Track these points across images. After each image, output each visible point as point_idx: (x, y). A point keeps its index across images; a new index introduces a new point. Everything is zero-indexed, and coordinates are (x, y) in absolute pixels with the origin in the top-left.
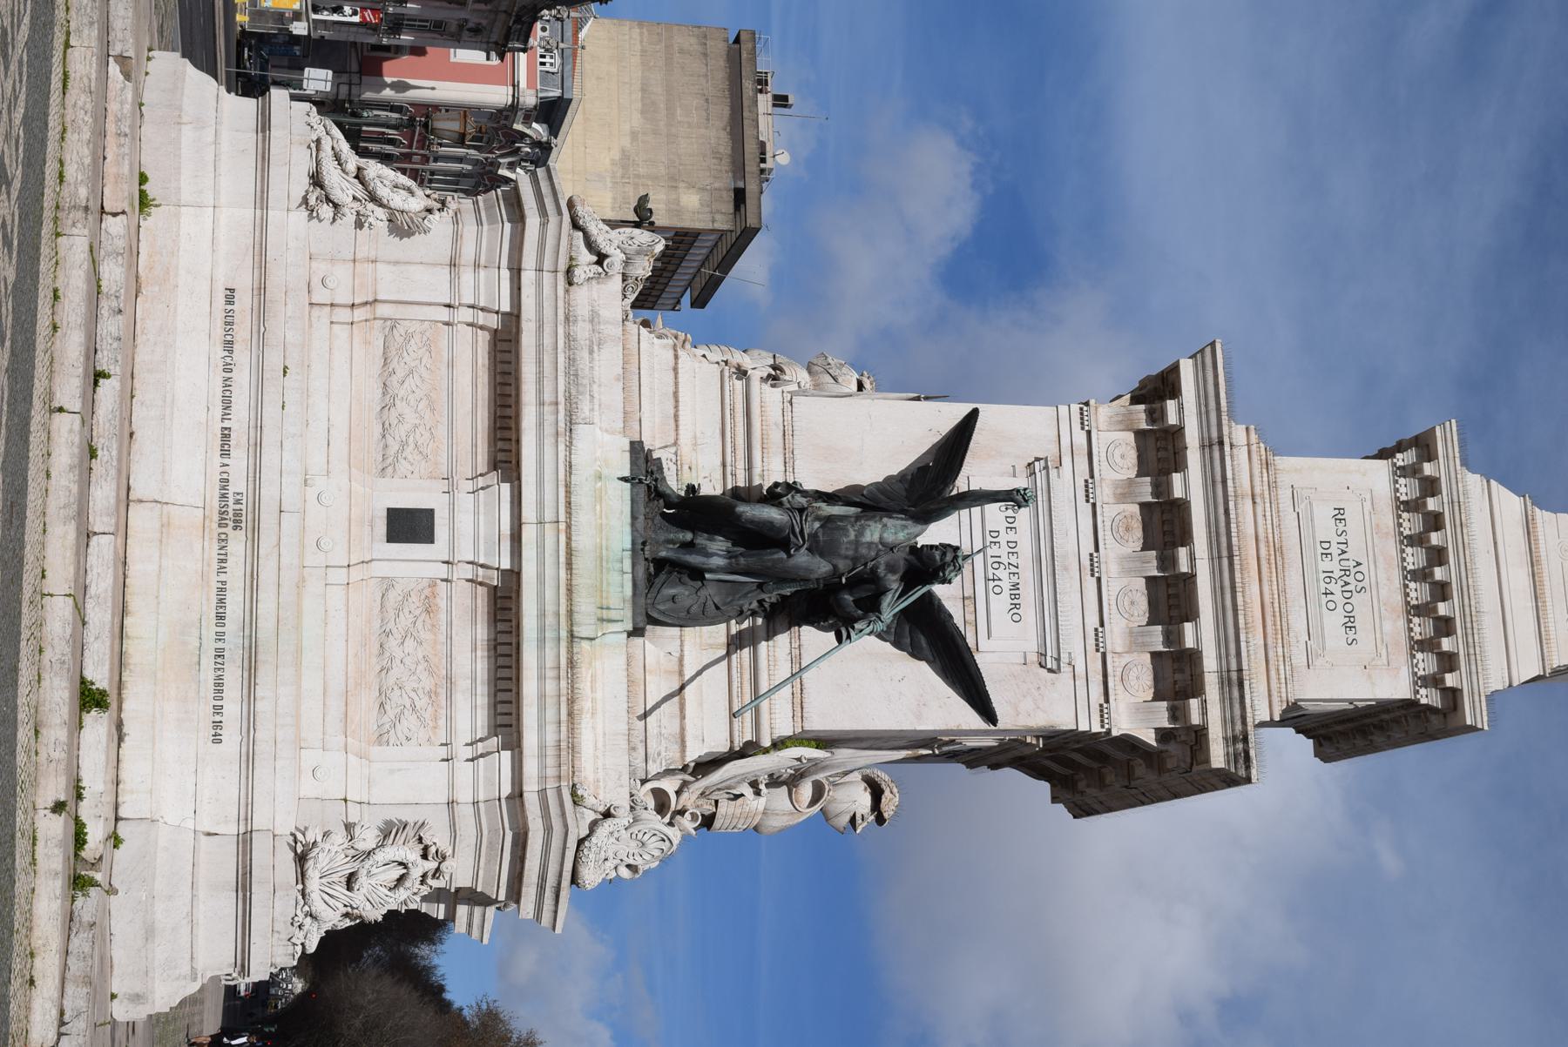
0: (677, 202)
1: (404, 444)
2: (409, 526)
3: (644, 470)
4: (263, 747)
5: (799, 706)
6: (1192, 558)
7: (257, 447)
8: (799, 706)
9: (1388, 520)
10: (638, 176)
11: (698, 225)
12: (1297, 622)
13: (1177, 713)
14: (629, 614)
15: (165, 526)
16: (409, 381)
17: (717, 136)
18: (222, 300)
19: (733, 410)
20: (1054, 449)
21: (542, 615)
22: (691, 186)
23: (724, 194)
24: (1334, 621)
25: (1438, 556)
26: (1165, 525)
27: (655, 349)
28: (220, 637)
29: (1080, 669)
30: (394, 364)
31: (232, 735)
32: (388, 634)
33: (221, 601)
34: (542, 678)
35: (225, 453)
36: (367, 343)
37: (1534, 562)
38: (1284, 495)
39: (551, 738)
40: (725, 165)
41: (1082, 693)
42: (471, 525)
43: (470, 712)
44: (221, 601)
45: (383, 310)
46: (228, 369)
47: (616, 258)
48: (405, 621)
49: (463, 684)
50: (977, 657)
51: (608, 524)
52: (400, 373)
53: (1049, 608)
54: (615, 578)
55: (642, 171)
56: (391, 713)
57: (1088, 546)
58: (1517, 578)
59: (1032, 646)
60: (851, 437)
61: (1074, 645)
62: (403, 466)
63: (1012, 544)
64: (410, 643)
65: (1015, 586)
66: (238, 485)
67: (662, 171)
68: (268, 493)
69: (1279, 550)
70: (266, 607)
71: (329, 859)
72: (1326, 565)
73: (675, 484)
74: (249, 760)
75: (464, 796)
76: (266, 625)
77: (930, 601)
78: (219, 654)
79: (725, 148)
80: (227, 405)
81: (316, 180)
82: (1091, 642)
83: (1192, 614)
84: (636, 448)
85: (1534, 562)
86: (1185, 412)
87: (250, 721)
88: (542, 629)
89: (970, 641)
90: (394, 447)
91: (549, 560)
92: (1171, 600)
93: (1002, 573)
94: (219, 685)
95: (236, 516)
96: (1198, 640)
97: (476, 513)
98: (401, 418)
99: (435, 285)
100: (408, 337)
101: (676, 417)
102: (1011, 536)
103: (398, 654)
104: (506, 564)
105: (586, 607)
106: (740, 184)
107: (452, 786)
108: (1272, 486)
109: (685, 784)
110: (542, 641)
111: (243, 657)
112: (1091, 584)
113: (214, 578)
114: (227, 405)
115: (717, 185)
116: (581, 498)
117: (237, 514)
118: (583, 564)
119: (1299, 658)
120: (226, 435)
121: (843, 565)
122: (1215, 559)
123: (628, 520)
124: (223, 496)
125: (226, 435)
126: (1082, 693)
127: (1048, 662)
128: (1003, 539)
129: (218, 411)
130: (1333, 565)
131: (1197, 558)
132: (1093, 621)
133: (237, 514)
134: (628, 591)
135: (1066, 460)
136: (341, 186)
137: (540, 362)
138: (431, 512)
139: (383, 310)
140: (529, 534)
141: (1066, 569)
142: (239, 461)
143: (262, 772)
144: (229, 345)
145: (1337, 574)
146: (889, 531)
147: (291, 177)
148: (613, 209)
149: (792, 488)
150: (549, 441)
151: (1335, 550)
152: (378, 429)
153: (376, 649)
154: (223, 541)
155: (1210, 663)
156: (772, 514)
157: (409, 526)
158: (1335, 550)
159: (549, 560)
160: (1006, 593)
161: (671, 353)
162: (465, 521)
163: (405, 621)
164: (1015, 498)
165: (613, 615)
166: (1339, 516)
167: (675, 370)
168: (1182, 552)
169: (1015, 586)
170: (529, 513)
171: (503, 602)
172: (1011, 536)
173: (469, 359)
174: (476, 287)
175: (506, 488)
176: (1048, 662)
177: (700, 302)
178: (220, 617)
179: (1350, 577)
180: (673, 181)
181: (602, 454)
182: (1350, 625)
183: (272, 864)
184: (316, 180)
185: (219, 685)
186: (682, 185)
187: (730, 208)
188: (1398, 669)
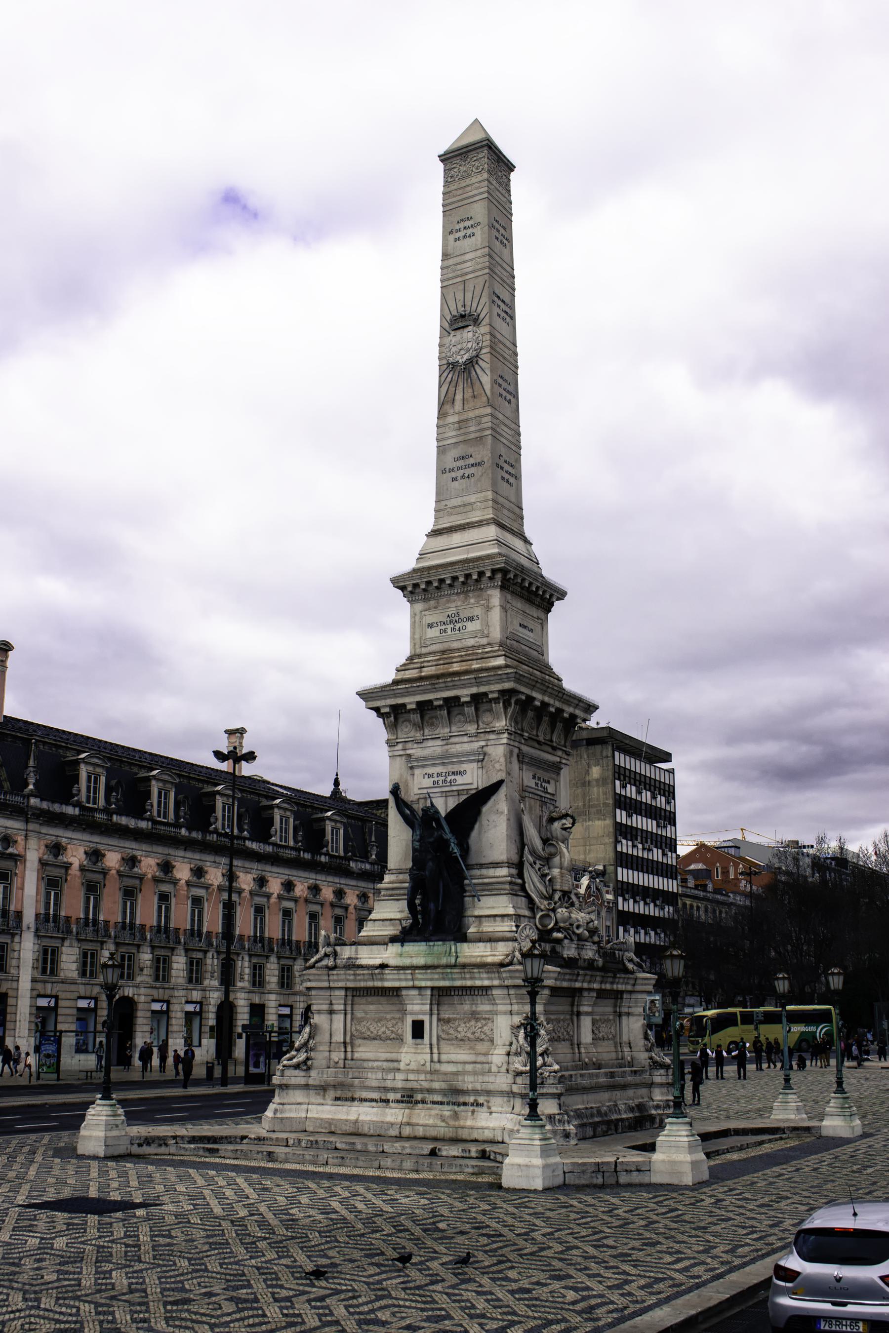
0: (597, 780)
1: (392, 1032)
2: (418, 1030)
4: (484, 1087)
5: (496, 865)
6: (436, 699)
7: (386, 1089)
8: (496, 865)
9: (432, 603)
10: (584, 805)
11: (611, 767)
12: (471, 642)
13: (496, 700)
14: (448, 943)
15: (409, 1124)
16: (372, 1029)
18: (338, 1103)
19: (391, 895)
20: (404, 758)
21: (444, 979)
22: (588, 773)
23: (590, 751)
24: (472, 626)
25: (442, 581)
28: (448, 1103)
29: (483, 743)
30: (366, 1036)
31: (481, 1100)
32: (457, 1038)
33: (437, 1103)
34: (465, 979)
35: (387, 1101)
36: (359, 1046)
38: (424, 650)
39: (485, 975)
41: (492, 742)
44: (437, 1103)
45: (348, 1040)
46: (362, 1100)
47: (329, 950)
48: (452, 1031)
49: (474, 1008)
50: (480, 788)
52: (369, 1033)
54: (436, 948)
56: (483, 1037)
57: (439, 742)
58: (457, 538)
59: (475, 765)
61: (476, 745)
62: (400, 1032)
63: (438, 775)
64: (460, 1029)
65: (453, 773)
66: (398, 1096)
67: (579, 791)
68: (399, 1085)
69: (443, 652)
70: (436, 1085)
72: (449, 631)
74: (488, 1093)
75: (509, 1008)
76: (444, 1085)
77: (452, 815)
78: (454, 1104)
80: (372, 1100)
81: (297, 1067)
82: (473, 739)
83: (457, 698)
84: (393, 940)
87: (476, 1092)
88: (449, 979)
89: (473, 792)
90: (393, 1036)
91: (425, 976)
93: (449, 779)
94: (464, 1104)
95: (409, 1098)
96: (467, 696)
97: (413, 1004)
98: (384, 1033)
99: (339, 1019)
100: (357, 1030)
101: (391, 920)
102: (435, 775)
103: (463, 1034)
104: (429, 992)
105: (444, 961)
106: (585, 742)
107: (505, 1013)
108: (420, 656)
109: (538, 908)
110: (453, 979)
111: (455, 1096)
112: (453, 740)
113: (429, 1106)
114: (372, 1100)
115: (585, 757)
116: (407, 962)
117: (408, 1096)
118: (430, 961)
119: (484, 641)
120: (382, 1101)
121: (429, 857)
122: (436, 690)
123: (416, 944)
124: (402, 1102)
125: (382, 1101)
126: (492, 742)
127: (482, 758)
128: (436, 779)
129: (374, 1104)
130: (449, 627)
131: (437, 696)
132: (465, 739)
133: (408, 1096)
134: (440, 943)
135: (408, 752)
136: (302, 1056)
137: (360, 980)
138: (413, 1021)
139: (348, 1040)
140: (418, 983)
141: (447, 751)
142: (391, 1096)
143: (491, 1087)
144: (353, 1099)
145: (452, 626)
147: (296, 1077)
148: (605, 820)
150: (385, 976)
151: (443, 627)
152: (389, 1042)
153: (462, 1043)
154: (417, 1102)
155: (474, 690)
157: (418, 1030)
158: (443, 627)
159: (425, 976)
160: (456, 777)
161: (369, 923)
162: (417, 1008)
163: (452, 1031)
165: (448, 950)
166: (430, 626)
167: (375, 920)
168: (436, 703)
169: (453, 773)
170: (410, 984)
172: (435, 775)
174: (338, 1004)
175: (404, 992)
176: (482, 758)
177: (666, 757)
178: (442, 1103)
179: (453, 620)
180: (585, 784)
182: (471, 619)
184: (297, 1067)
185: (464, 1104)
186: (587, 779)
187: (598, 748)
188: (489, 595)
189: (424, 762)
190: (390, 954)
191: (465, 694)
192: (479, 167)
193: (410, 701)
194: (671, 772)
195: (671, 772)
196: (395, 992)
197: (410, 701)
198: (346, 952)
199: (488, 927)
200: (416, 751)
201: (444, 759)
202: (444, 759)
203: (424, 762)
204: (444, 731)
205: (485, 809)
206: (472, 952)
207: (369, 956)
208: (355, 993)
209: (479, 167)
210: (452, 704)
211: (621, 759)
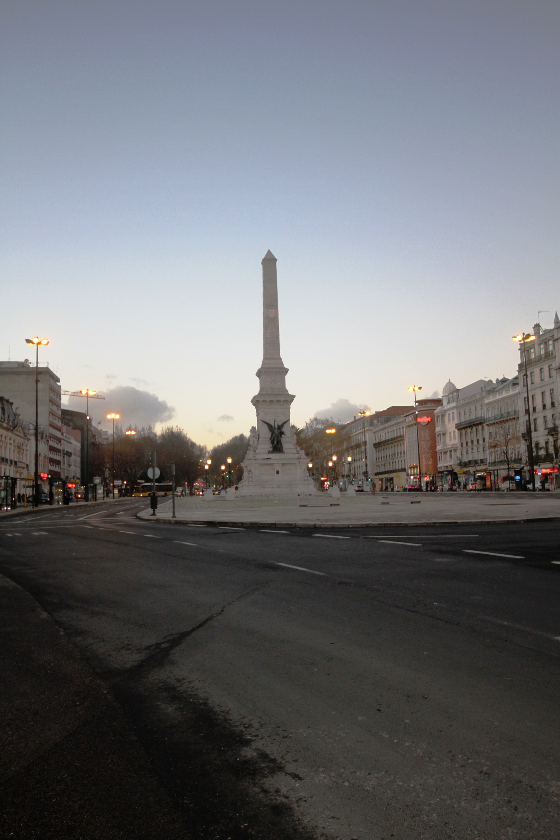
2: (278, 472)
27: (257, 452)
37: (271, 359)
71: (306, 478)
73: (271, 449)
86: (261, 400)
95: (279, 486)
131: (275, 399)
146: (276, 431)
149: (271, 439)
156: (275, 442)
157: (278, 472)
171: (284, 464)
181: (270, 456)
183: (306, 482)
191: (282, 400)
192: (269, 263)
193: (268, 400)
194: (60, 386)
195: (60, 386)
196: (272, 464)
197: (268, 400)
205: (285, 425)
208: (261, 464)
209: (269, 263)
211: (51, 381)
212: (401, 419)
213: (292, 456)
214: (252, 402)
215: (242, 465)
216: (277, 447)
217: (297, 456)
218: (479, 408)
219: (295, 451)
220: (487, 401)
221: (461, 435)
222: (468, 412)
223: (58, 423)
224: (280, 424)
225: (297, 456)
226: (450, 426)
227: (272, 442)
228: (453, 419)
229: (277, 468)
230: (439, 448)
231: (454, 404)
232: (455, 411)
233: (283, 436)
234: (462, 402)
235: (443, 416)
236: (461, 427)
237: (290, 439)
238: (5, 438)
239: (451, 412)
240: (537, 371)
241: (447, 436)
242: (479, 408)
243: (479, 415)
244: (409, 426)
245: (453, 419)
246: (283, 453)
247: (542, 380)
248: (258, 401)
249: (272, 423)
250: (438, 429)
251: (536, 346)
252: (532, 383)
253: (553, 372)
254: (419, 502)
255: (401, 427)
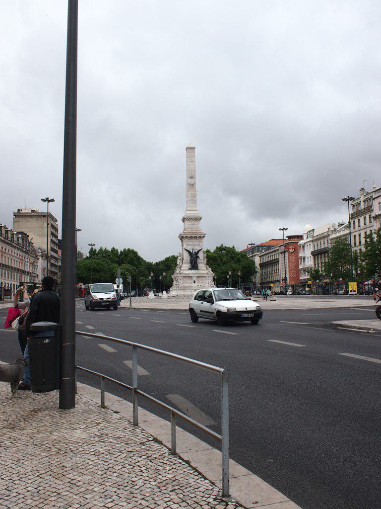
2: (194, 282)
3: (190, 269)
17: (33, 220)
26: (191, 237)
37: (191, 210)
40: (39, 219)
42: (194, 279)
43: (204, 279)
51: (194, 271)
53: (196, 245)
55: (41, 233)
58: (192, 212)
60: (186, 256)
61: (198, 243)
71: (212, 285)
73: (191, 267)
79: (36, 218)
85: (191, 210)
86: (184, 236)
92: (196, 237)
131: (193, 236)
157: (194, 282)
164: (193, 250)
171: (198, 277)
173: (187, 279)
180: (42, 227)
181: (190, 271)
189: (190, 245)
190: (187, 272)
191: (198, 236)
193: (189, 236)
196: (191, 277)
197: (189, 236)
198: (182, 271)
199: (202, 268)
200: (188, 243)
201: (193, 245)
202: (193, 245)
203: (190, 245)
204: (193, 241)
206: (201, 272)
207: (185, 272)
208: (184, 277)
210: (196, 237)
212: (277, 248)
213: (204, 272)
214: (179, 237)
215: (173, 277)
216: (194, 266)
217: (206, 272)
218: (326, 242)
219: (205, 268)
220: (331, 237)
221: (315, 259)
222: (319, 244)
223: (56, 248)
224: (196, 251)
225: (206, 272)
226: (307, 253)
227: (191, 263)
228: (310, 248)
229: (194, 279)
230: (301, 267)
231: (310, 239)
232: (311, 243)
233: (198, 259)
234: (316, 238)
235: (303, 247)
236: (315, 254)
237: (203, 261)
238: (24, 258)
239: (308, 244)
240: (362, 218)
241: (306, 259)
242: (326, 242)
243: (326, 246)
244: (281, 253)
245: (310, 248)
246: (199, 269)
247: (365, 224)
248: (183, 237)
249: (191, 251)
250: (300, 255)
251: (362, 203)
252: (359, 226)
253: (372, 219)
254: (275, 300)
255: (277, 253)
